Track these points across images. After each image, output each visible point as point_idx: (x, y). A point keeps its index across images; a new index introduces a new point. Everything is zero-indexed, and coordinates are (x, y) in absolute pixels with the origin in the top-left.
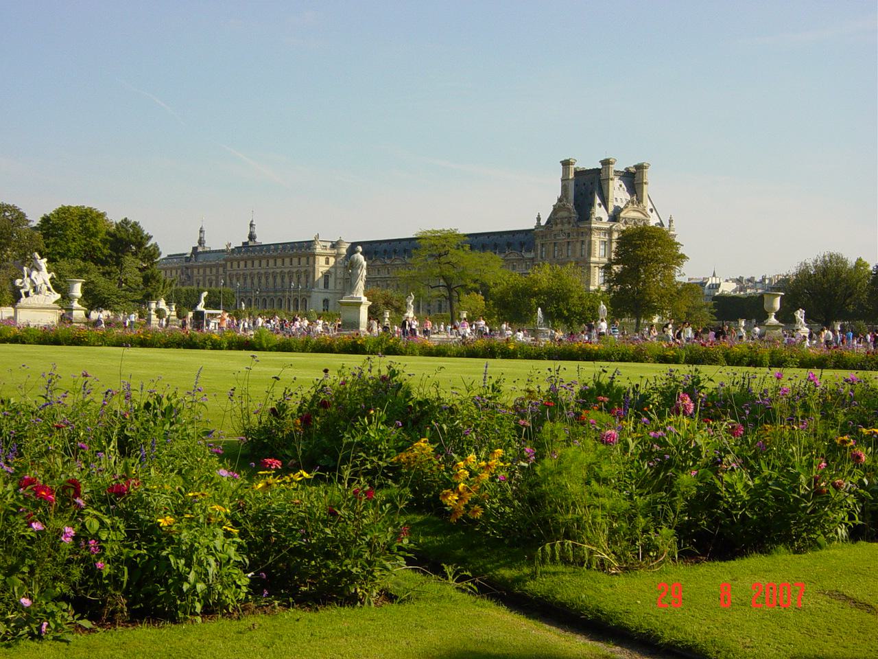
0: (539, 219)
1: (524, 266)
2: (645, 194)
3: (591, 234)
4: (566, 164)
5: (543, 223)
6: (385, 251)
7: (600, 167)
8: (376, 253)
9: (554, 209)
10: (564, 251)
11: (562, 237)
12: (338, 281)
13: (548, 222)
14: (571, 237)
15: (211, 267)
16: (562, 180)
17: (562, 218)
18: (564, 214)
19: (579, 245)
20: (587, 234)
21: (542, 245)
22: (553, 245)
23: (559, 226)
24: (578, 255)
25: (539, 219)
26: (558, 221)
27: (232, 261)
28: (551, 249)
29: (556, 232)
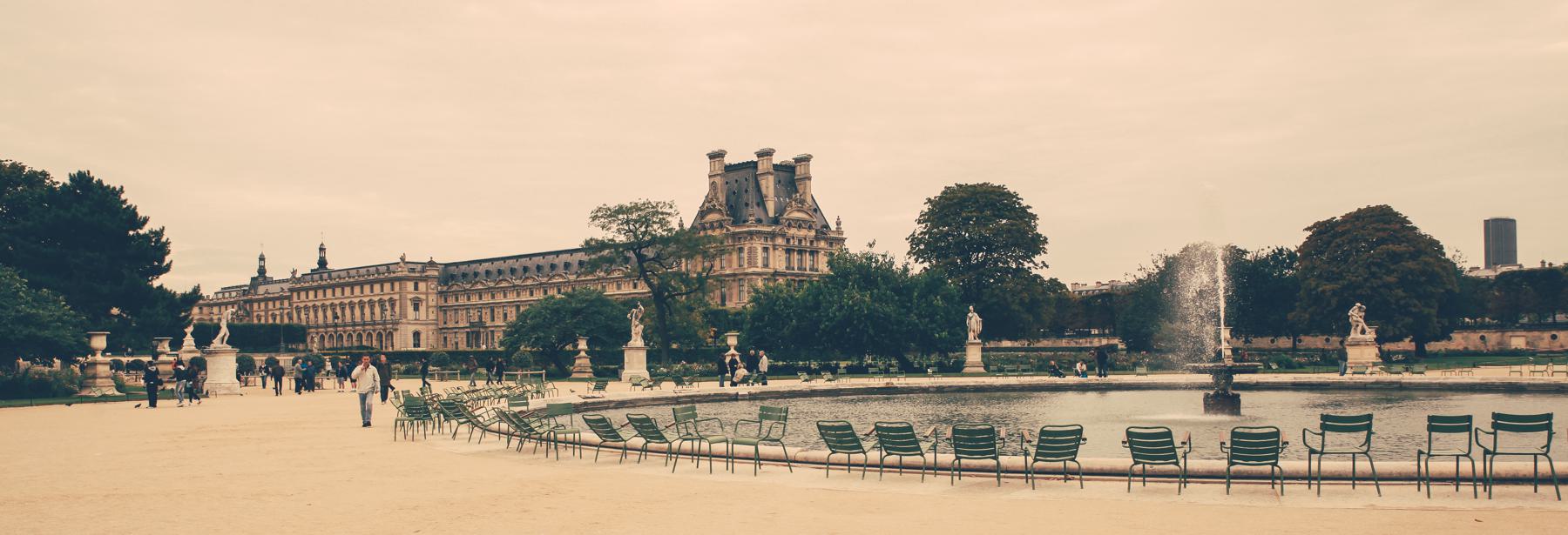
15: (274, 300)
19: (735, 256)
24: (735, 265)
27: (298, 291)
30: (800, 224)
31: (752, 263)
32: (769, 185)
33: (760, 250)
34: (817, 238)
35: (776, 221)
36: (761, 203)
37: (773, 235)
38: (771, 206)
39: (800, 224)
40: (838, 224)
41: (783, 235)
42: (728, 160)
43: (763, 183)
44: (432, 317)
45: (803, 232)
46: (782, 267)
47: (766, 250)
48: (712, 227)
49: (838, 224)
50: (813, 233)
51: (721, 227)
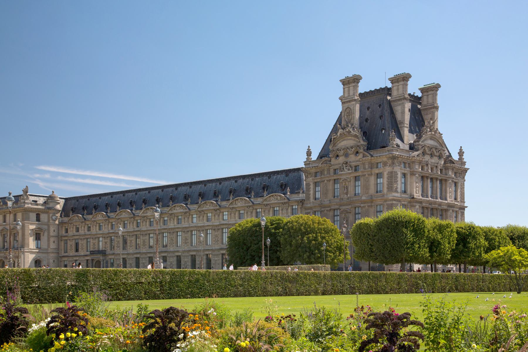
0: (309, 153)
1: (289, 210)
5: (314, 157)
6: (107, 205)
8: (96, 207)
10: (351, 189)
11: (346, 171)
12: (52, 240)
13: (321, 157)
14: (361, 169)
19: (372, 179)
20: (385, 164)
21: (316, 184)
22: (331, 182)
23: (341, 159)
25: (309, 153)
28: (330, 187)
29: (336, 167)
31: (391, 188)
33: (399, 175)
40: (461, 153)
42: (363, 87)
44: (53, 246)
45: (435, 160)
46: (418, 195)
47: (404, 175)
49: (461, 153)
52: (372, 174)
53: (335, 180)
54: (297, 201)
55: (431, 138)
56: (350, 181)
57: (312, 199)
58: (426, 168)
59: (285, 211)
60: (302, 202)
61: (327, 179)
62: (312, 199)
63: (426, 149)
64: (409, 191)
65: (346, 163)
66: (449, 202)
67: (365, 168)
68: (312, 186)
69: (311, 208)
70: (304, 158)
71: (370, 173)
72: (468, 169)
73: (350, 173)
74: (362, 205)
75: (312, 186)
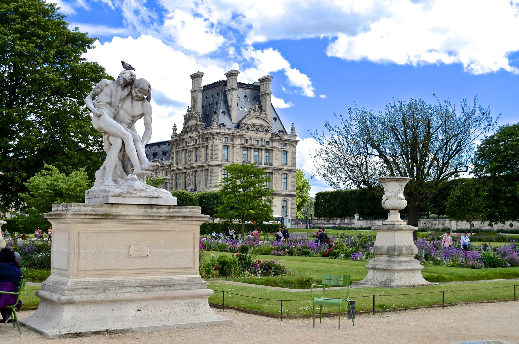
0: (175, 129)
2: (268, 104)
3: (213, 139)
4: (196, 77)
5: (179, 132)
7: (225, 79)
9: (185, 119)
16: (192, 92)
17: (191, 127)
18: (192, 122)
19: (203, 150)
21: (177, 152)
23: (190, 134)
24: (203, 159)
25: (175, 129)
26: (188, 129)
30: (257, 128)
32: (236, 98)
33: (220, 147)
34: (272, 140)
35: (238, 126)
36: (228, 111)
37: (233, 137)
38: (234, 113)
39: (257, 128)
41: (241, 137)
43: (229, 96)
45: (260, 135)
47: (226, 147)
48: (191, 131)
50: (269, 136)
51: (196, 130)
52: (203, 147)
53: (186, 150)
54: (167, 166)
55: (256, 118)
56: (193, 151)
57: (175, 165)
58: (249, 141)
59: (161, 173)
60: (170, 165)
61: (182, 149)
62: (175, 165)
63: (250, 127)
64: (230, 159)
65: (191, 138)
66: (274, 166)
67: (199, 142)
68: (175, 155)
69: (174, 171)
70: (171, 132)
71: (202, 145)
72: (298, 141)
73: (192, 145)
74: (198, 170)
75: (175, 155)
